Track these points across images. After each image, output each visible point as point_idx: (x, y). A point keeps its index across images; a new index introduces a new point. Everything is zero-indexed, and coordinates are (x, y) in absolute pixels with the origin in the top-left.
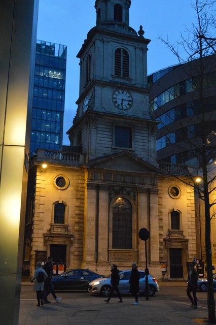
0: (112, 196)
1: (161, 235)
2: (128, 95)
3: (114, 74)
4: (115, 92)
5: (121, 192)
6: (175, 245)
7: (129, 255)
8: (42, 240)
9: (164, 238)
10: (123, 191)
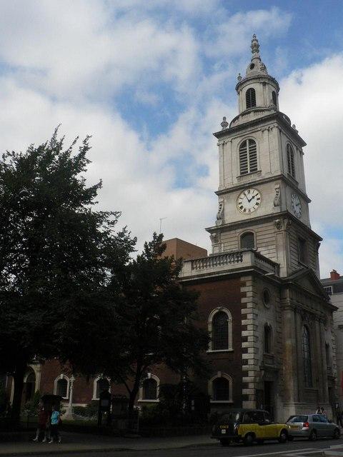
2: (256, 192)
3: (239, 175)
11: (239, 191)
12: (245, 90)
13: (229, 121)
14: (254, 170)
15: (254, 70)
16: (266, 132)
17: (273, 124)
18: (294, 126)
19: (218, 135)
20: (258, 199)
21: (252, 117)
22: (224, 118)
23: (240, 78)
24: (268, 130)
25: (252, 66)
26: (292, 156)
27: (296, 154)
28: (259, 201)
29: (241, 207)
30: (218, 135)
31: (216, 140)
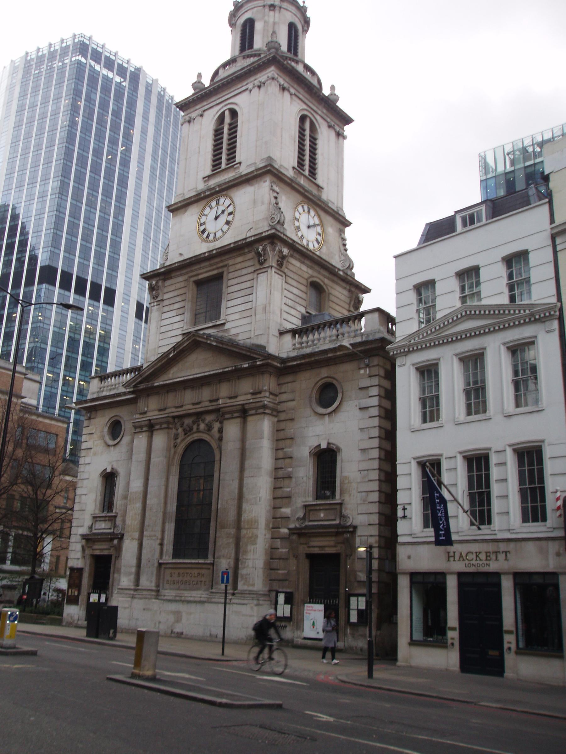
0: (179, 441)
1: (276, 521)
2: (228, 202)
4: (203, 209)
5: (195, 427)
6: (324, 545)
7: (199, 574)
8: (78, 547)
9: (292, 526)
10: (198, 425)
11: (203, 203)
13: (206, 82)
16: (256, 89)
20: (230, 214)
24: (259, 87)
26: (313, 141)
28: (230, 218)
29: (203, 231)
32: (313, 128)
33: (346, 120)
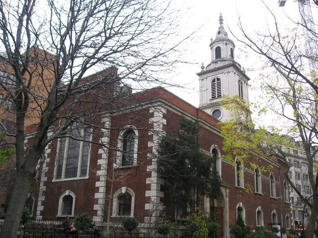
3: (211, 98)
12: (215, 48)
13: (205, 66)
14: (219, 96)
15: (220, 35)
17: (231, 69)
18: (243, 68)
19: (199, 75)
21: (220, 64)
22: (203, 64)
23: (212, 40)
25: (219, 33)
27: (244, 85)
30: (199, 75)
31: (198, 77)
32: (241, 84)
33: (248, 79)
